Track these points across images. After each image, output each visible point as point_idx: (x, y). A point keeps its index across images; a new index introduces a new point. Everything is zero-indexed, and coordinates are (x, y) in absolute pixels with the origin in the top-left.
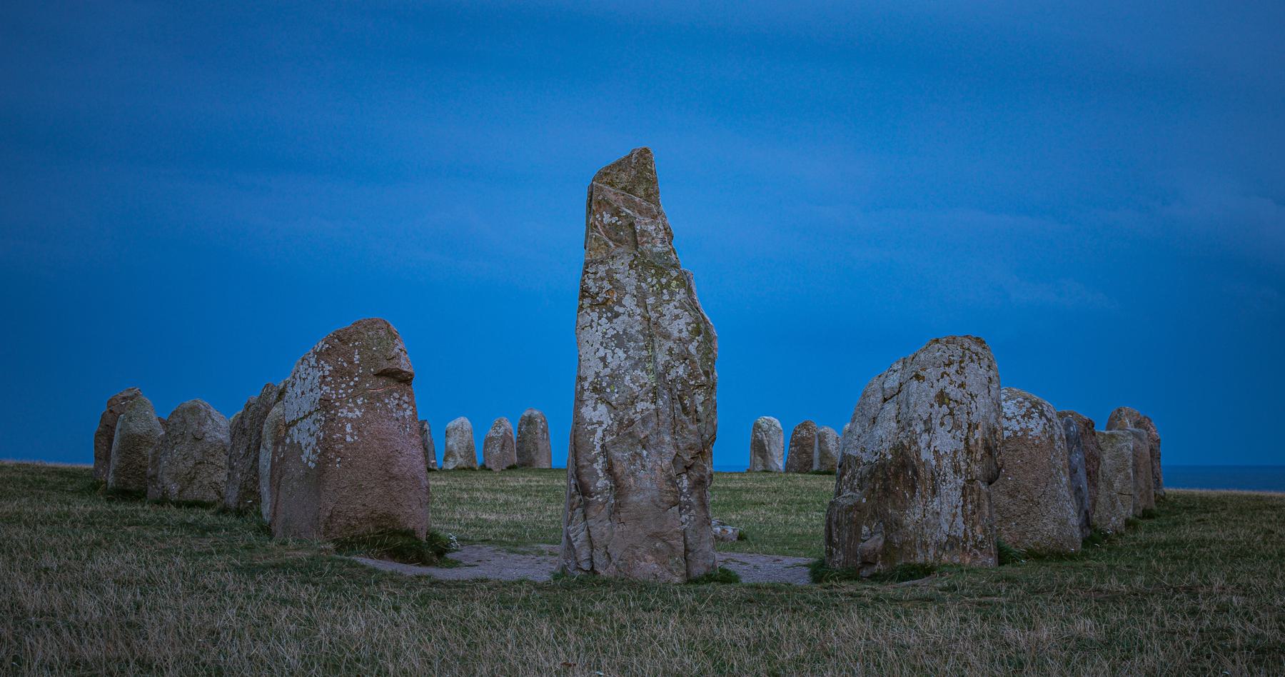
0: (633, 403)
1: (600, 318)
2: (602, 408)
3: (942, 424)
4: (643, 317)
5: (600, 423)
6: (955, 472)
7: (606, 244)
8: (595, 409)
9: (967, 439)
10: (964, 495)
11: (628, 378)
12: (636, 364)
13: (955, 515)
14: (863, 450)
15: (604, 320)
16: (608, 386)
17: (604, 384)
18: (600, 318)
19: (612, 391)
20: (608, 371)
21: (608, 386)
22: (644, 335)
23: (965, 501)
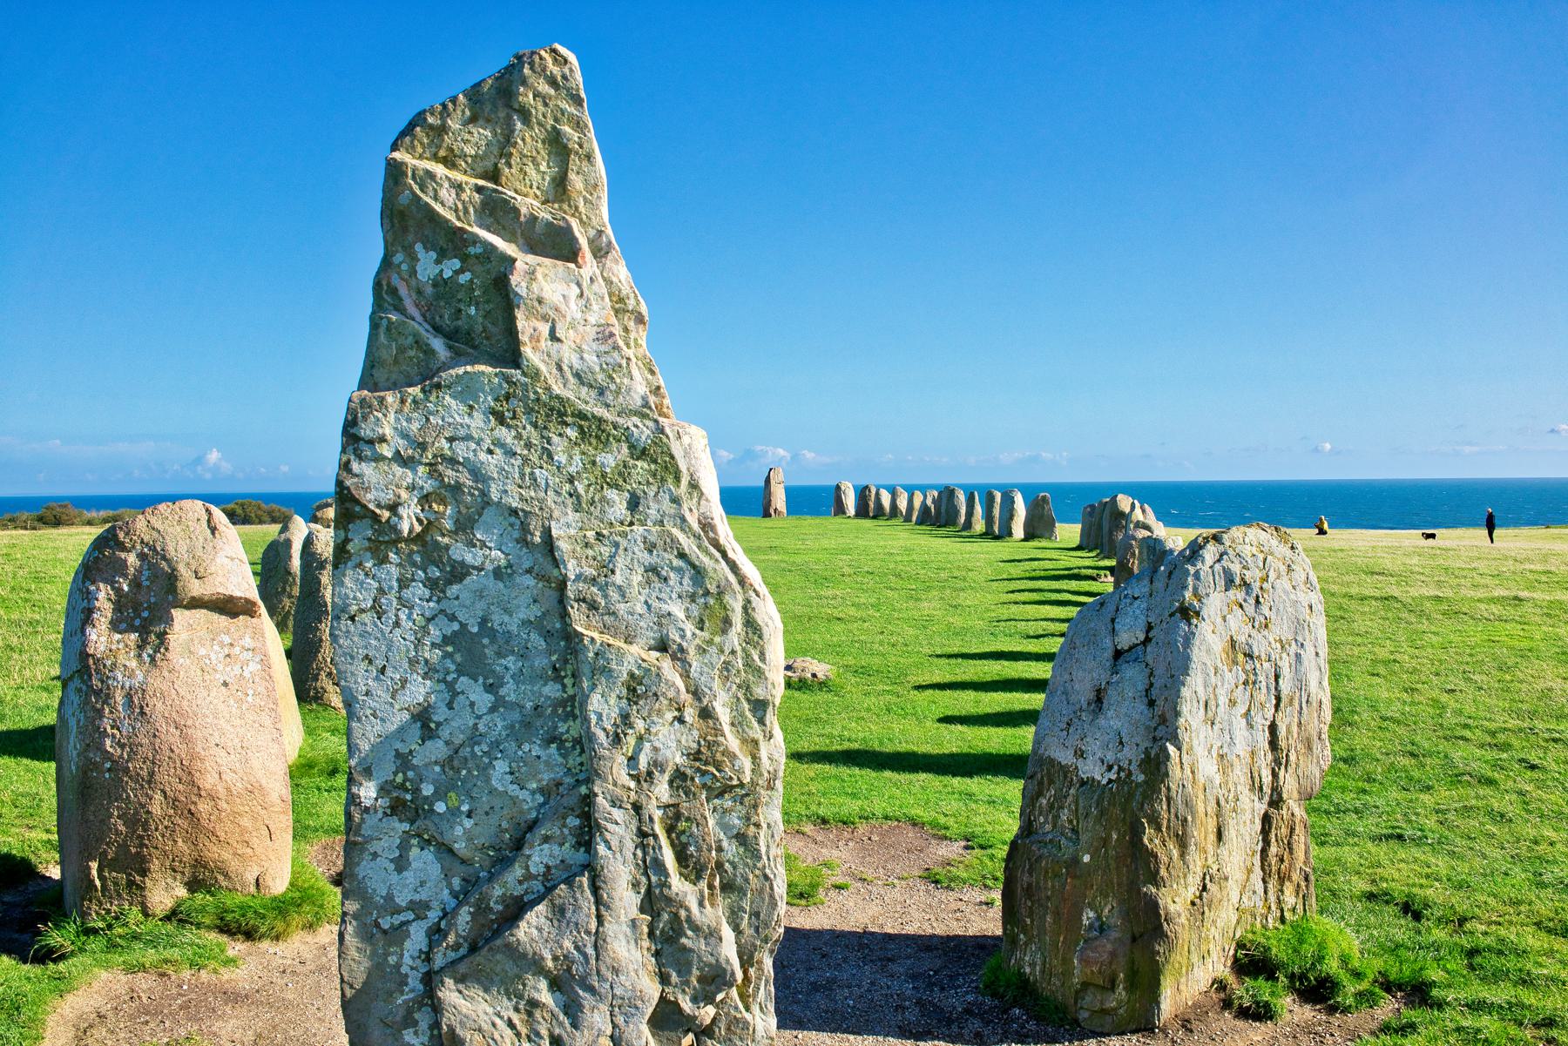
0: (518, 845)
1: (403, 583)
2: (423, 861)
3: (1233, 703)
4: (541, 577)
5: (419, 908)
6: (1252, 789)
7: (418, 343)
8: (401, 864)
9: (1273, 728)
10: (1265, 832)
11: (501, 766)
12: (527, 725)
13: (1250, 871)
14: (1080, 754)
15: (418, 591)
16: (440, 794)
17: (427, 790)
18: (403, 583)
19: (454, 812)
20: (437, 749)
21: (440, 794)
22: (548, 635)
23: (1267, 842)
